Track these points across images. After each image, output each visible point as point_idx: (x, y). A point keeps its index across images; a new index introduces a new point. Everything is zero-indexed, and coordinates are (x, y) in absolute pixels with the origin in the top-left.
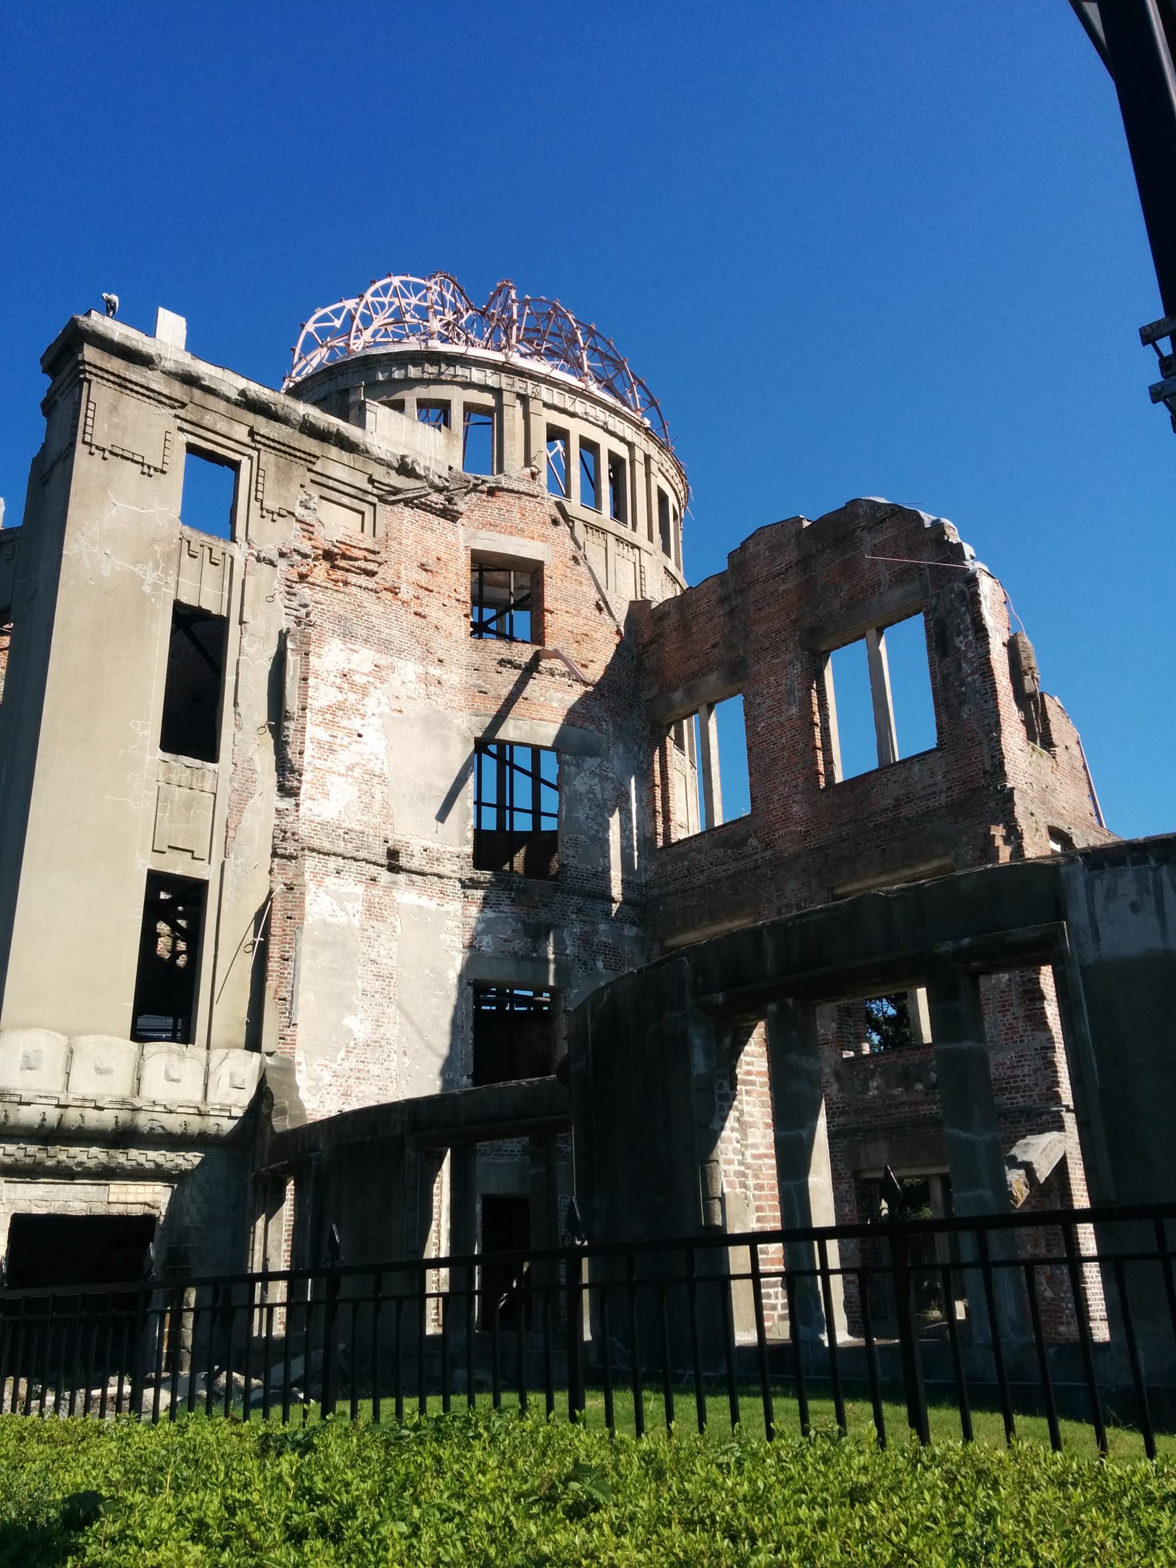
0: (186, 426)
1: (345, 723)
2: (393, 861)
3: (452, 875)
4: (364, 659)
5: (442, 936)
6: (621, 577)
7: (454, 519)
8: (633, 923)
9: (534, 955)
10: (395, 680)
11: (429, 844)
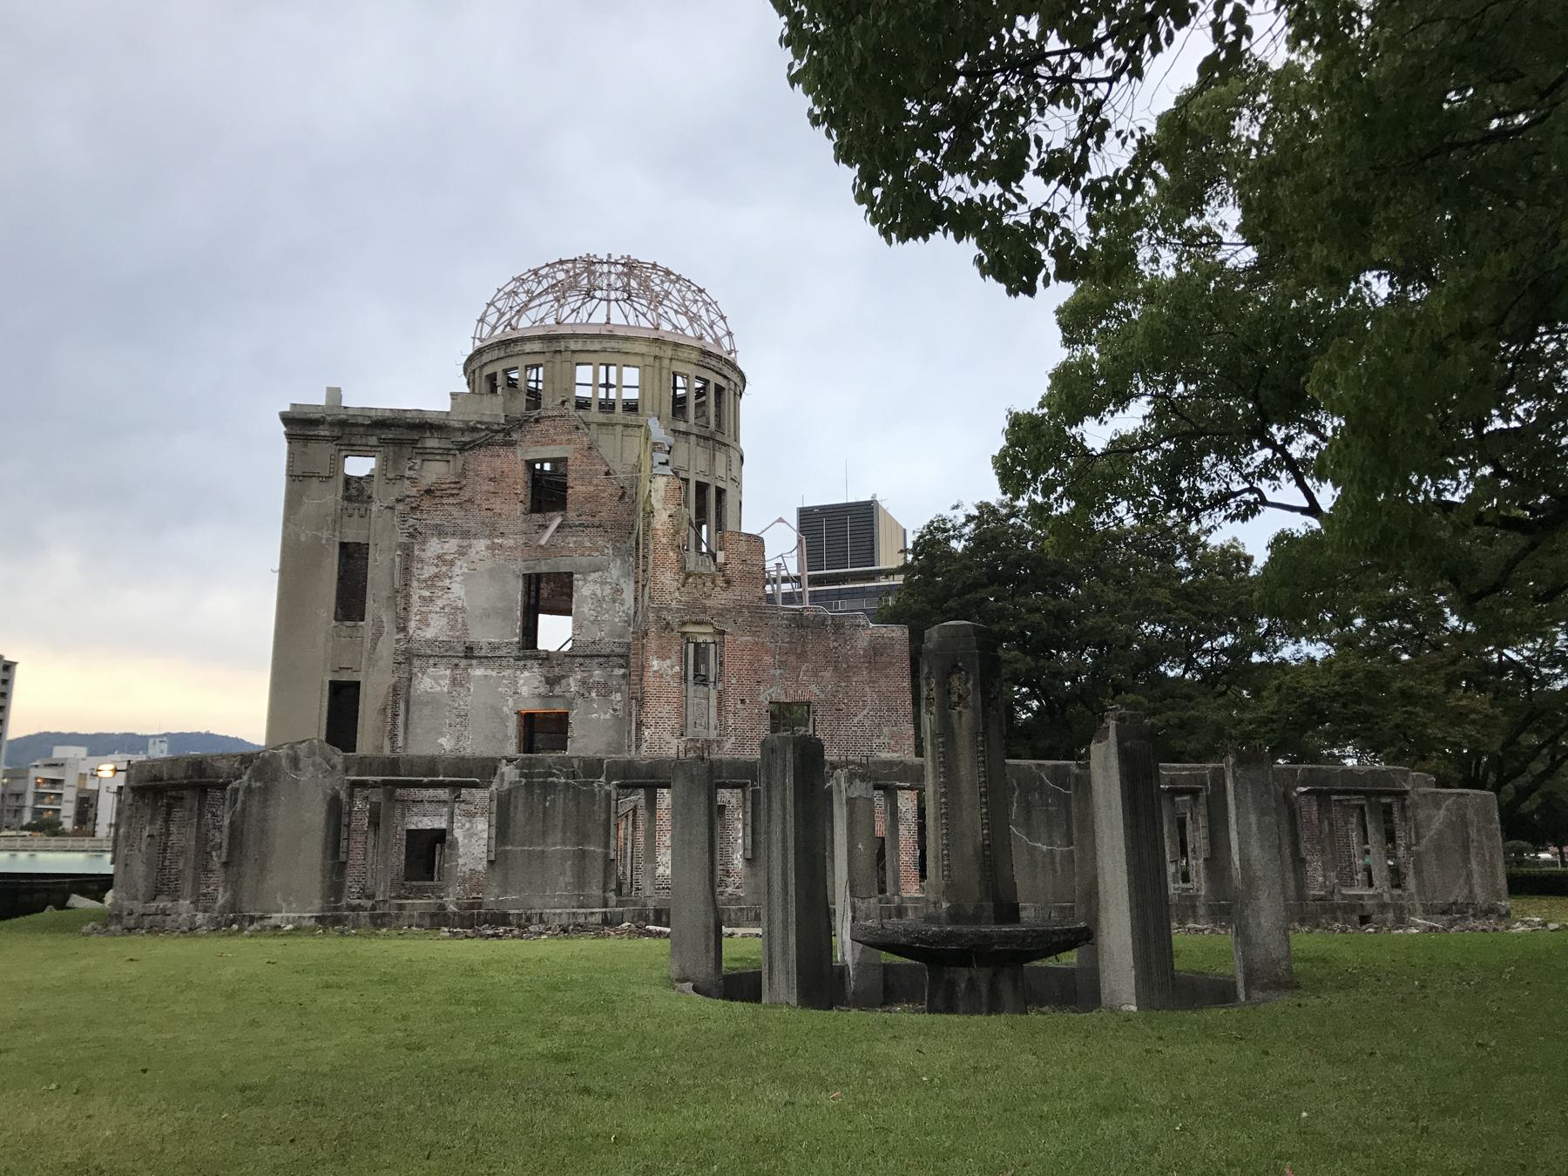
1: (440, 584)
2: (469, 652)
4: (452, 545)
7: (512, 445)
8: (622, 667)
10: (472, 552)
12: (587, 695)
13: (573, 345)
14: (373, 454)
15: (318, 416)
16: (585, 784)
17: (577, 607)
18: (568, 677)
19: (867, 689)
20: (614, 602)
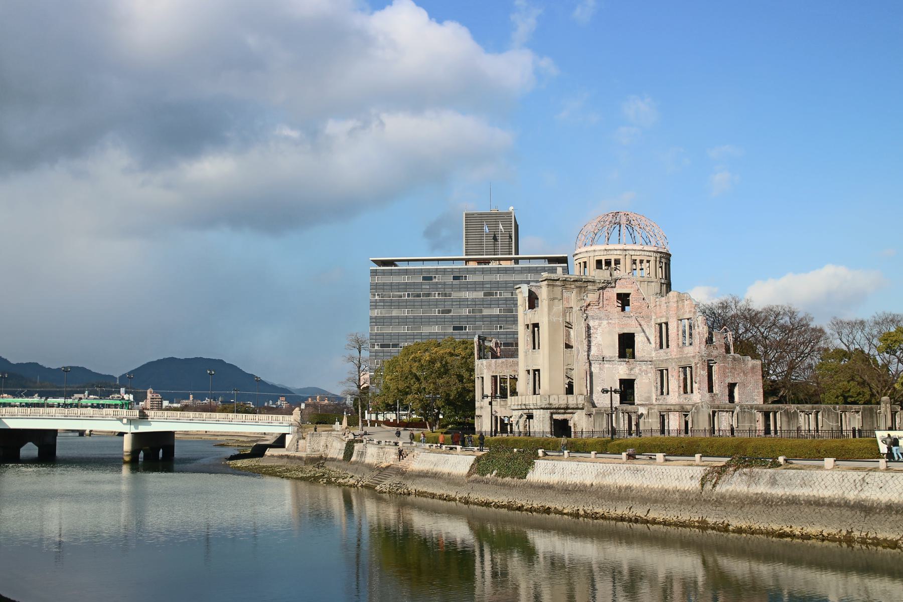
4: (597, 322)
8: (650, 365)
10: (602, 325)
13: (633, 253)
17: (637, 345)
19: (751, 379)
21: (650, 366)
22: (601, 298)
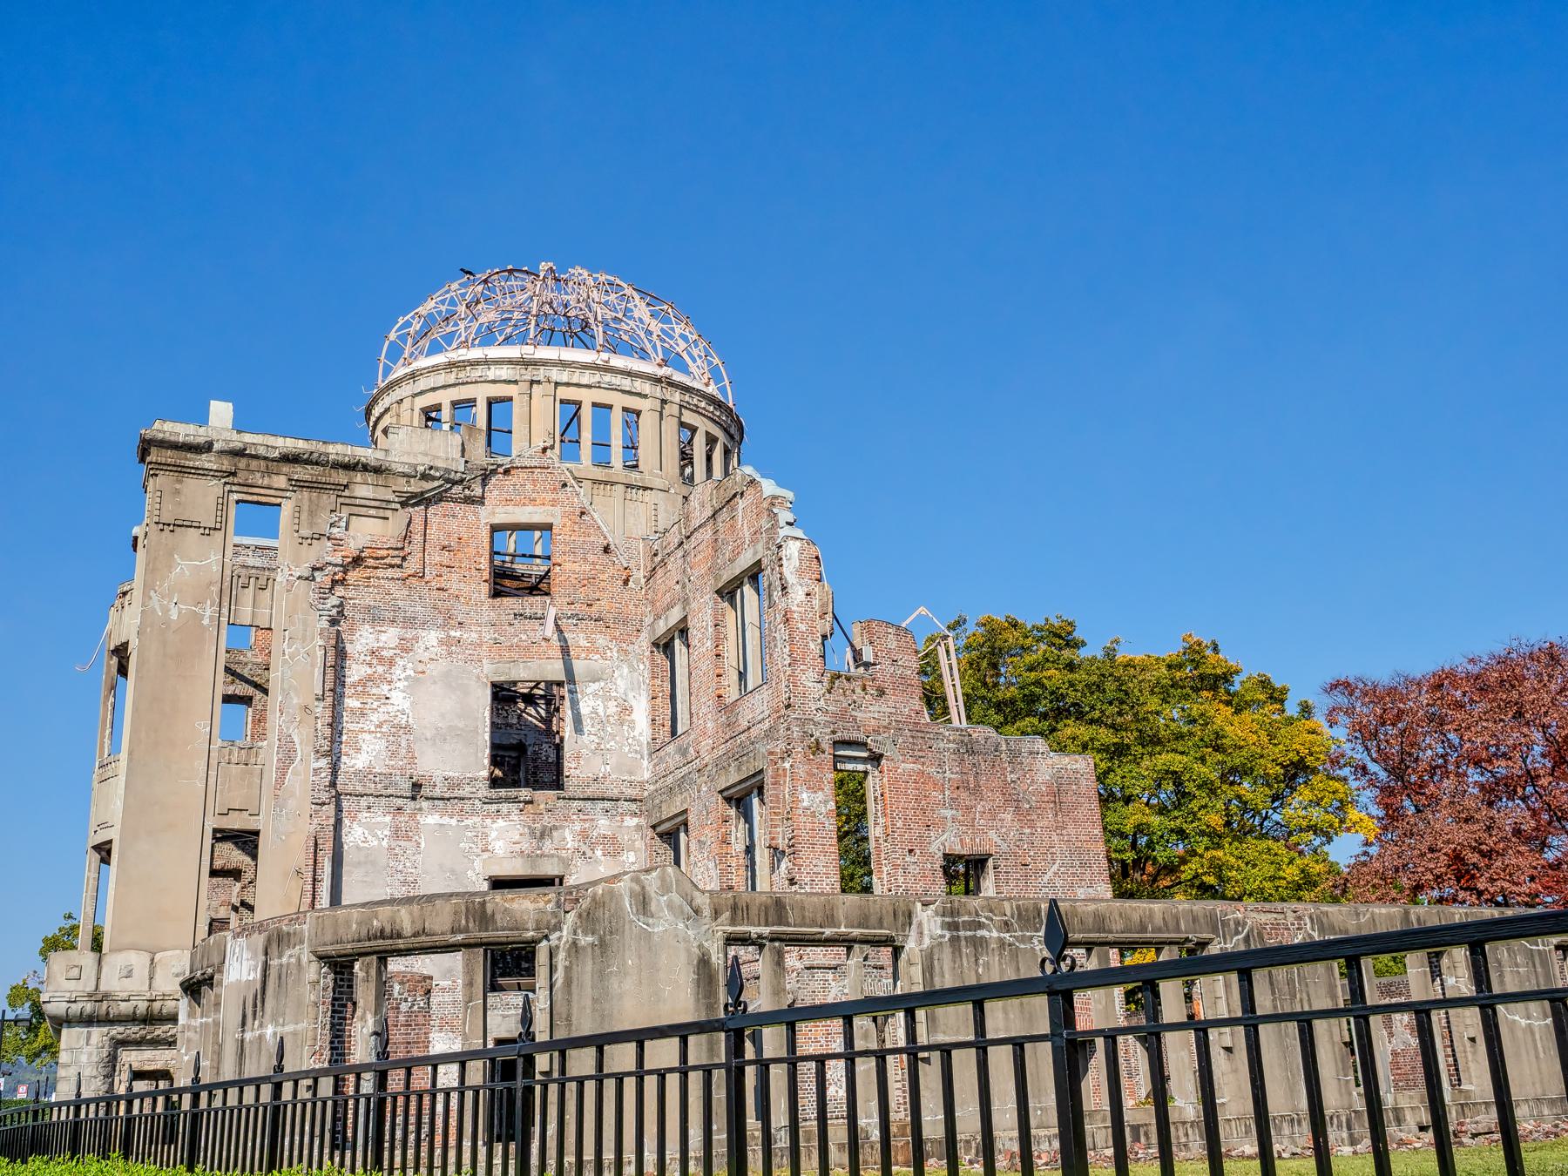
0: (234, 488)
1: (374, 691)
3: (472, 796)
5: (461, 845)
6: (631, 520)
9: (538, 852)
10: (419, 648)
11: (451, 774)
12: (589, 853)
13: (556, 374)
14: (279, 500)
15: (201, 440)
16: (1022, 939)
18: (562, 827)
19: (1055, 837)
20: (622, 724)
21: (632, 822)
22: (418, 538)
